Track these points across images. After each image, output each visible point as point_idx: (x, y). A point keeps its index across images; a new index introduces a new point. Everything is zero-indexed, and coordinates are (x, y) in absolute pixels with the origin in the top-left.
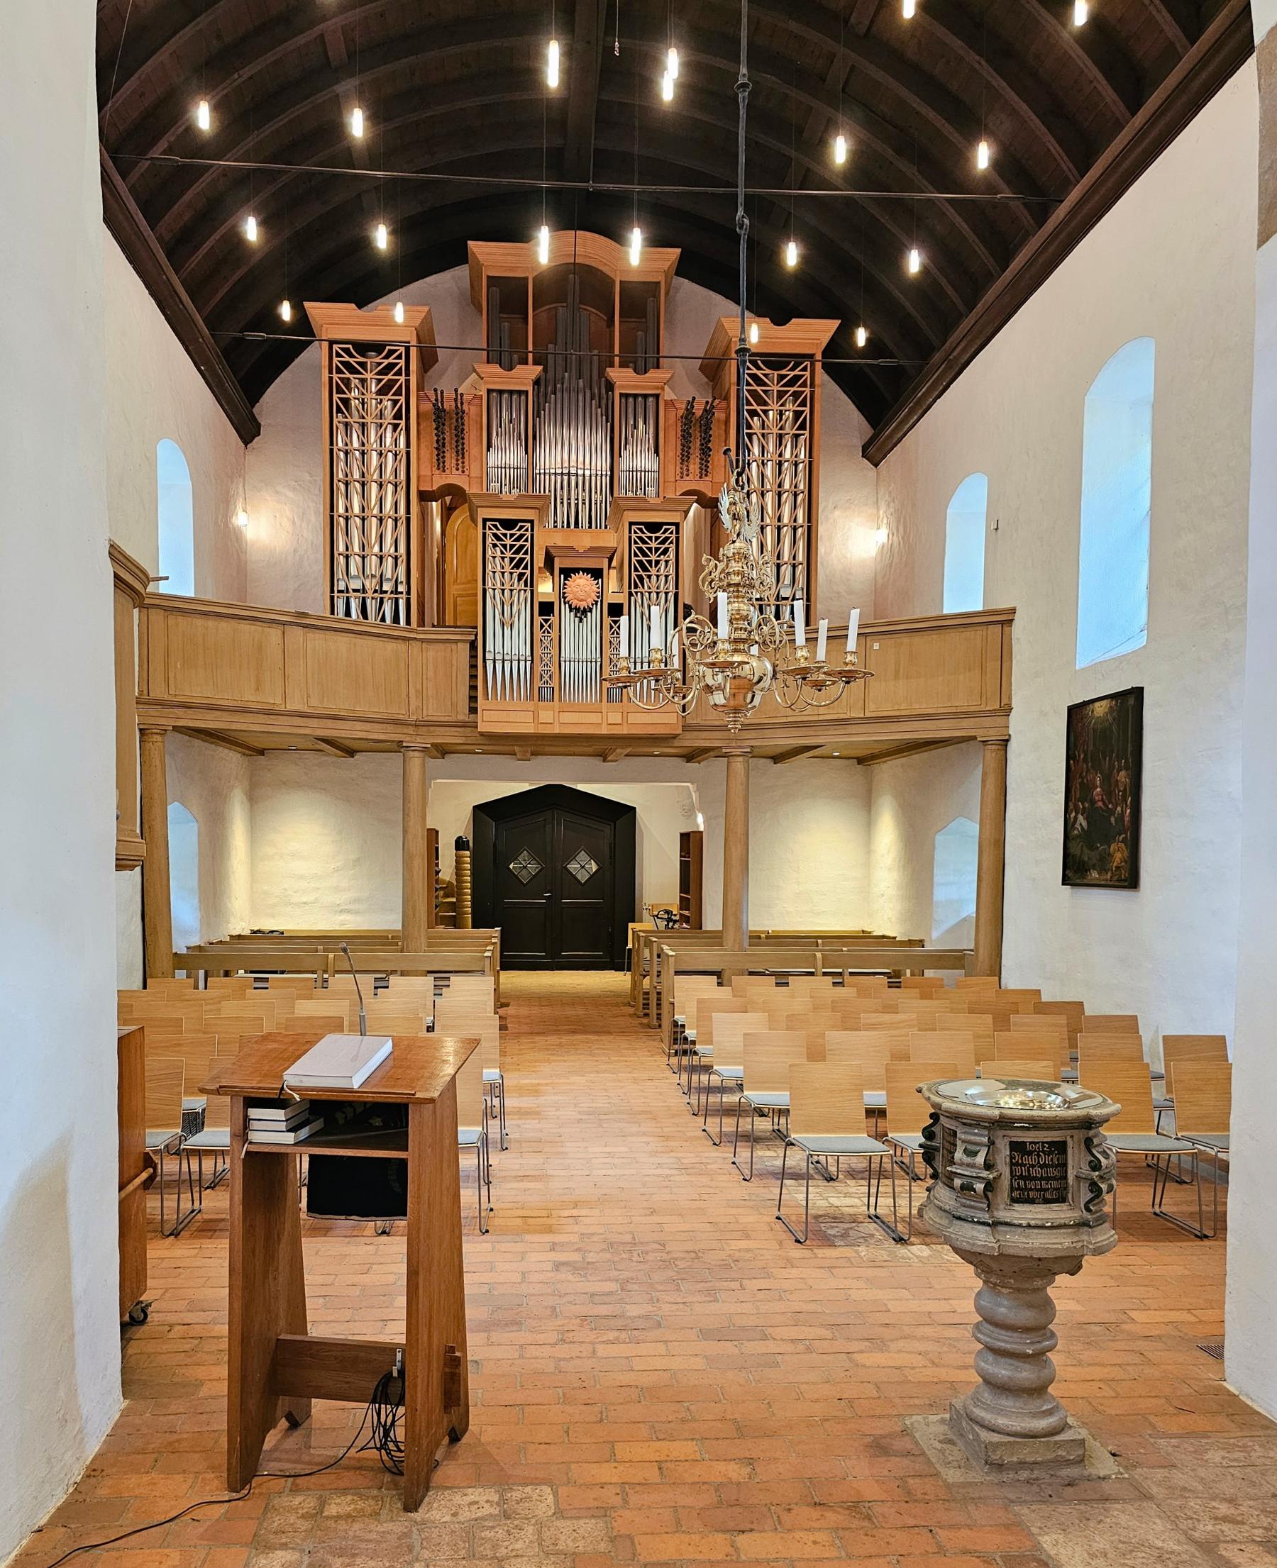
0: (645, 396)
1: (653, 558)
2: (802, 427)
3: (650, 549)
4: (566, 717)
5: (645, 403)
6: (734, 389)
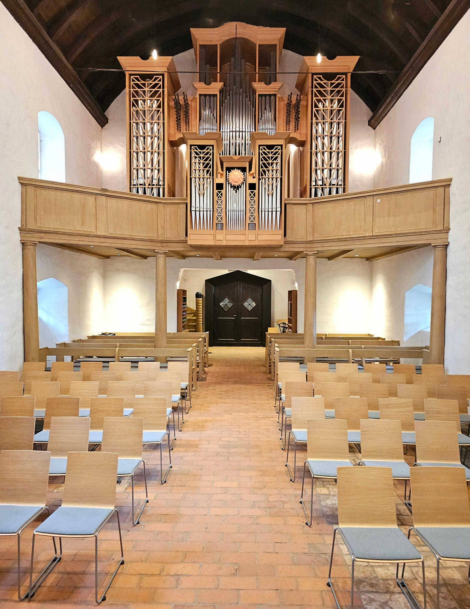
0: (270, 95)
1: (270, 161)
2: (342, 106)
3: (269, 157)
4: (229, 237)
5: (269, 99)
6: (310, 90)
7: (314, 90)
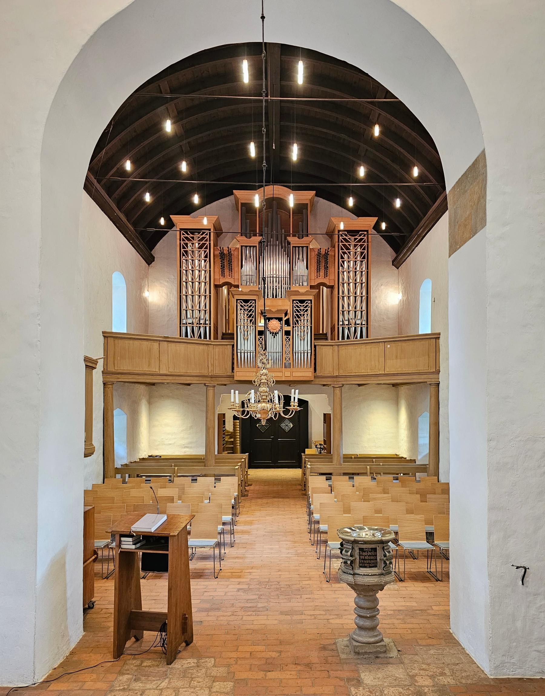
1: (302, 313)
2: (364, 258)
3: (301, 310)
7: (340, 244)
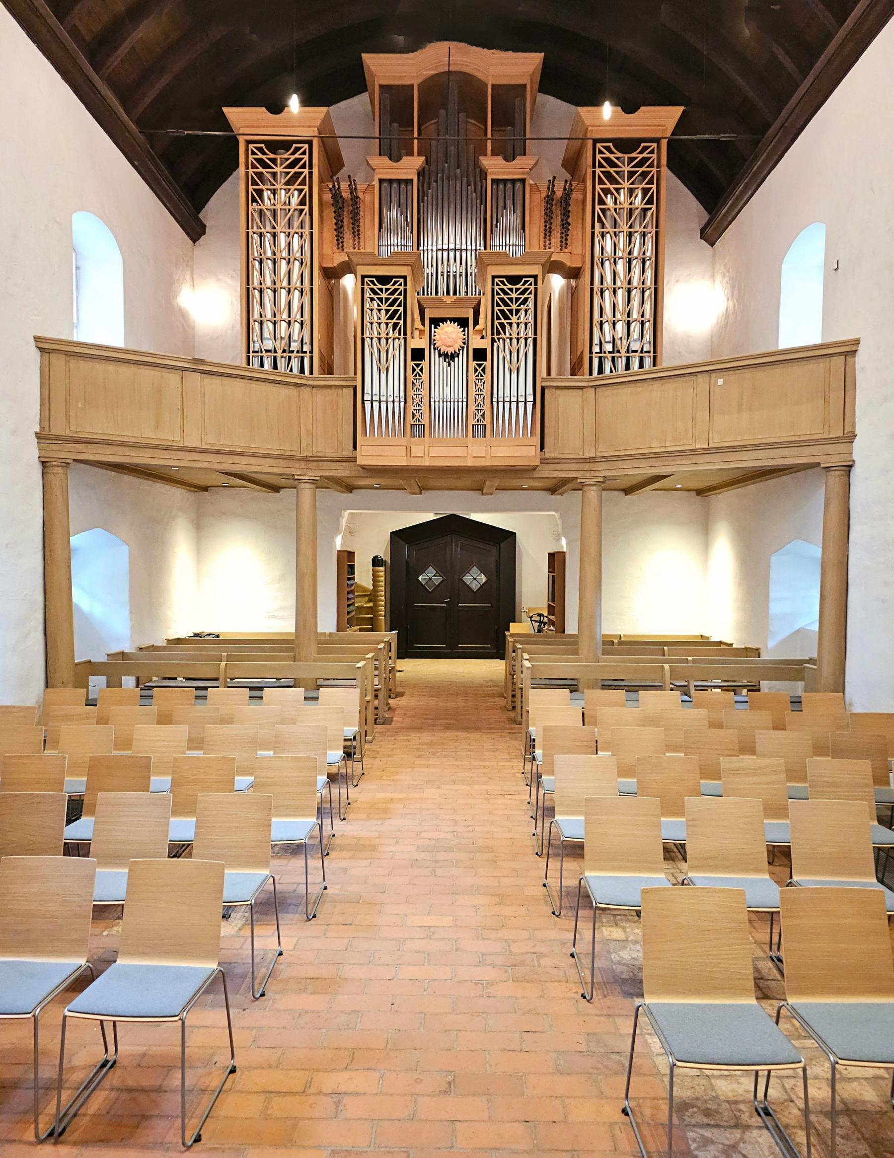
1: (514, 307)
3: (511, 299)
